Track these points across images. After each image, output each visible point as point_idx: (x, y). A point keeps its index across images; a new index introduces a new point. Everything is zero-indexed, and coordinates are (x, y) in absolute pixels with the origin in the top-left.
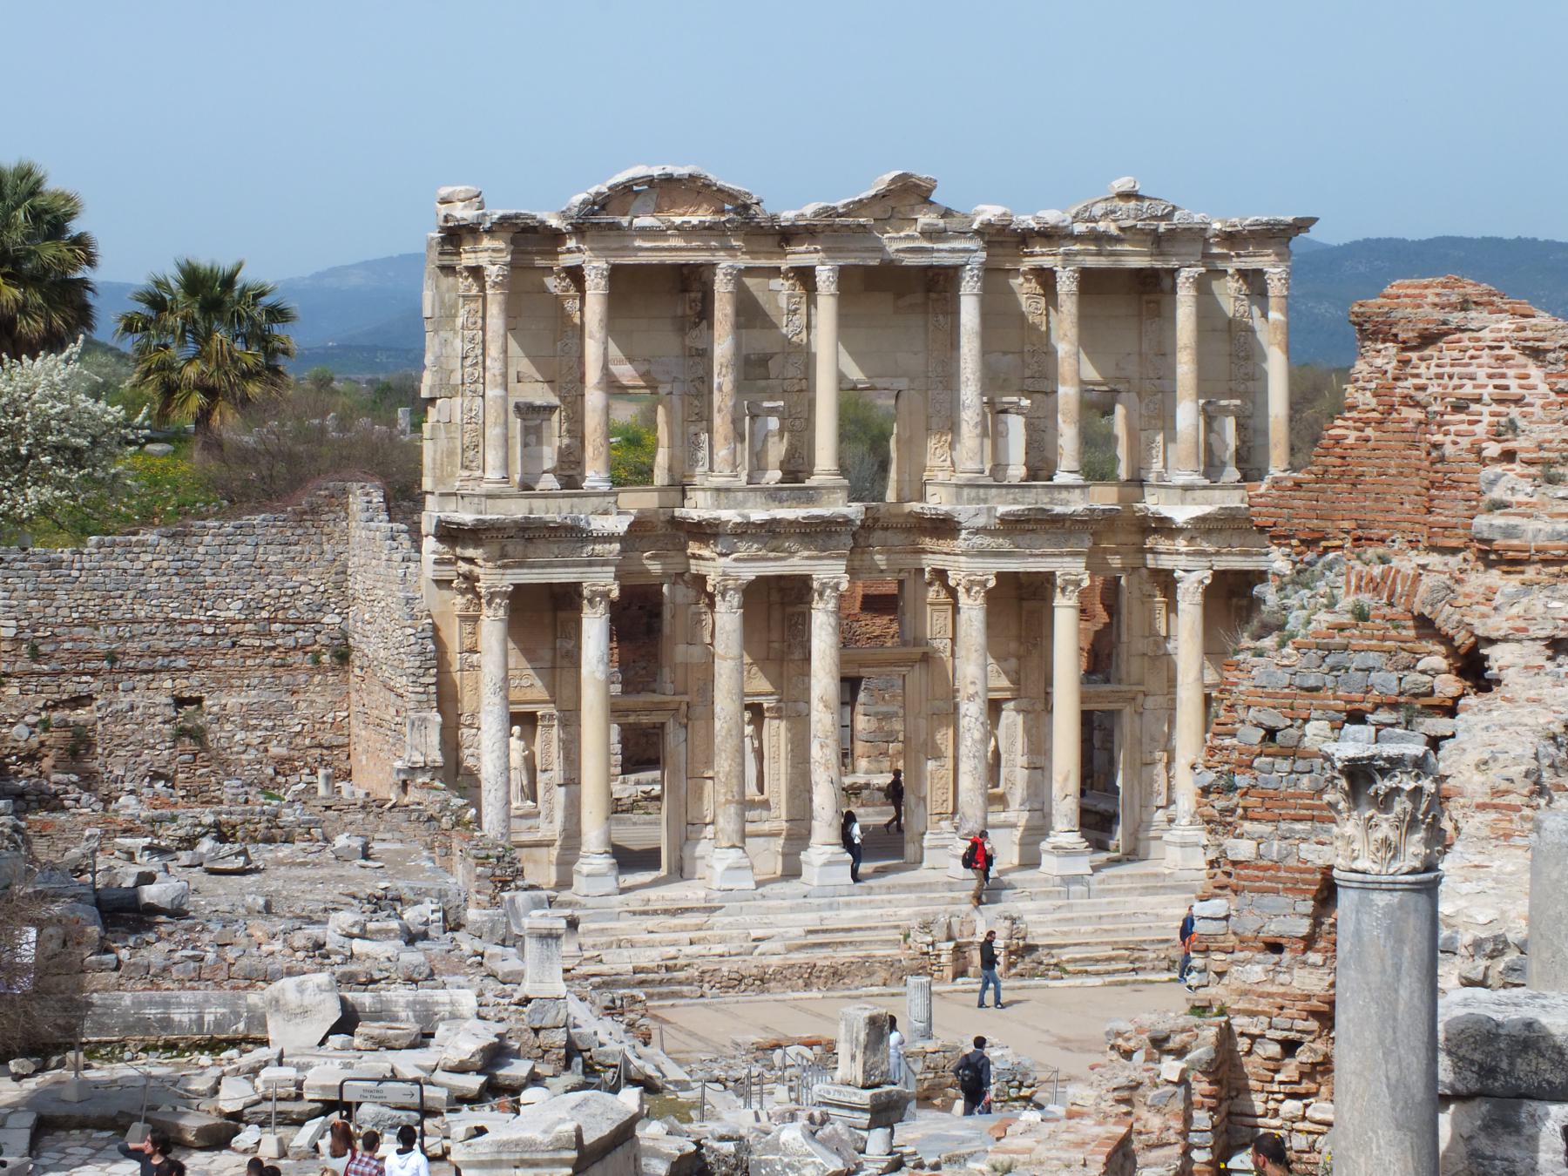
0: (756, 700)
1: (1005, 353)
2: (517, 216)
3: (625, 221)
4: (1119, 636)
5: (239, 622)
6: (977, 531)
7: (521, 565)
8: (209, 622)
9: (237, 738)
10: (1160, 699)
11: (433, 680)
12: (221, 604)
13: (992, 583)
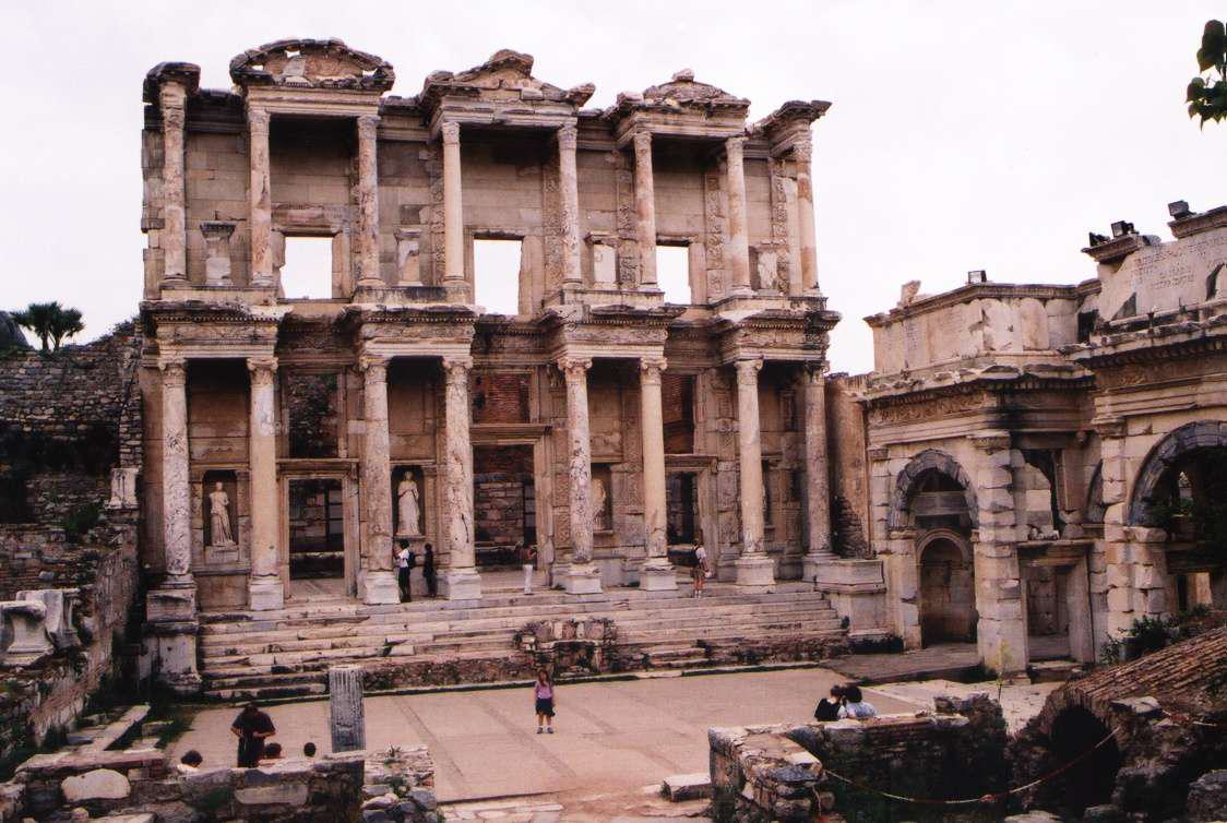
0: (416, 462)
1: (603, 211)
2: (181, 65)
3: (277, 78)
4: (697, 418)
5: (50, 423)
6: (576, 325)
7: (191, 341)
8: (28, 424)
9: (48, 507)
10: (730, 464)
11: (138, 443)
12: (38, 411)
13: (589, 365)
